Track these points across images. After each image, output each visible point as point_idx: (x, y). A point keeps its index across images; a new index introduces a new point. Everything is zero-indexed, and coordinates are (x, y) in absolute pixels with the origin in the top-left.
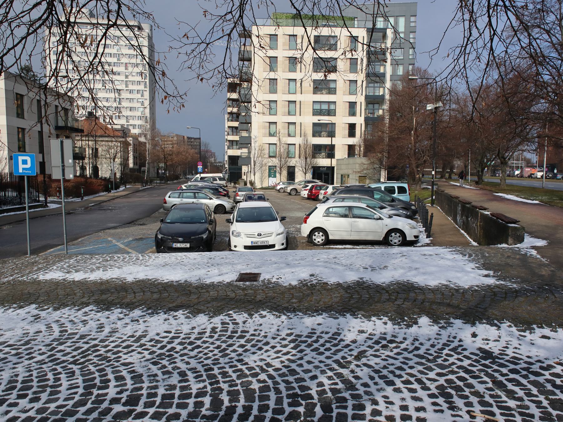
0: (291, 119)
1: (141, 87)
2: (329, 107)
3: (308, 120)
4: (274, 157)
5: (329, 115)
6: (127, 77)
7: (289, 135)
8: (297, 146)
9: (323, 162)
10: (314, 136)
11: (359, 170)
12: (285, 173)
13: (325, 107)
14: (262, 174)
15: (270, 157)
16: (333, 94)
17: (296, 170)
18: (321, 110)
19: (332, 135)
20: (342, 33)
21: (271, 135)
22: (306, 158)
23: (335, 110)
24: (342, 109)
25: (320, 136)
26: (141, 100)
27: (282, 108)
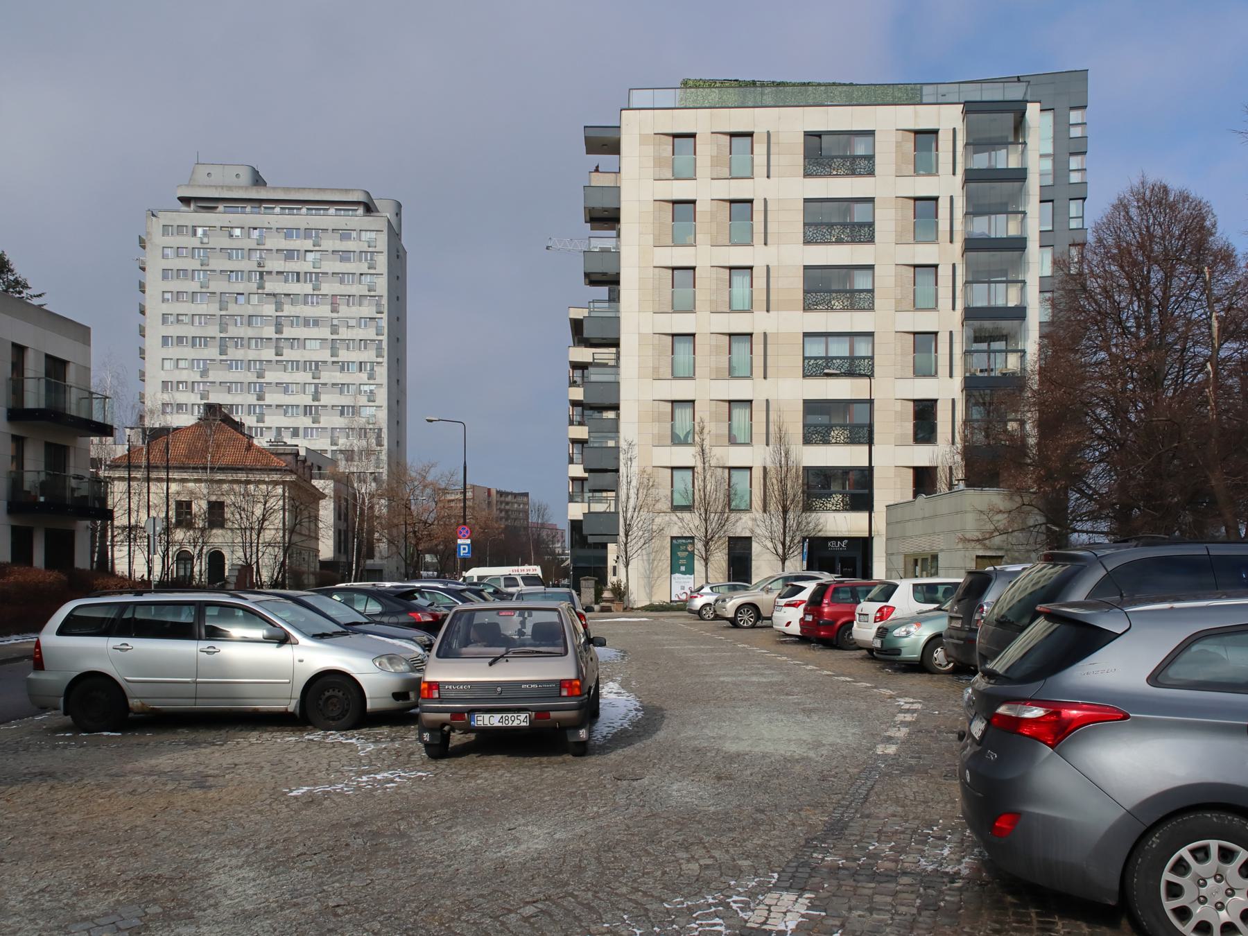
0: (739, 390)
1: (369, 355)
2: (852, 349)
3: (790, 391)
4: (688, 508)
5: (851, 374)
6: (334, 330)
7: (732, 441)
8: (757, 474)
9: (840, 523)
10: (807, 441)
11: (978, 535)
12: (720, 558)
13: (839, 349)
14: (651, 562)
15: (675, 508)
16: (864, 309)
17: (756, 547)
18: (828, 359)
19: (864, 435)
20: (889, 123)
21: (676, 441)
22: (785, 511)
23: (872, 358)
24: (891, 357)
25: (826, 441)
26: (366, 388)
27: (708, 355)
